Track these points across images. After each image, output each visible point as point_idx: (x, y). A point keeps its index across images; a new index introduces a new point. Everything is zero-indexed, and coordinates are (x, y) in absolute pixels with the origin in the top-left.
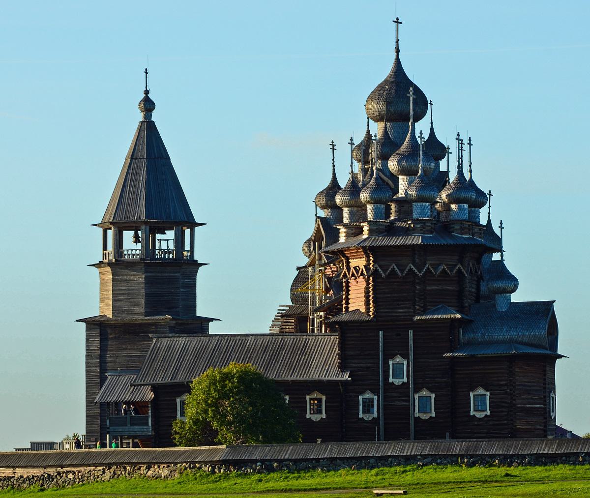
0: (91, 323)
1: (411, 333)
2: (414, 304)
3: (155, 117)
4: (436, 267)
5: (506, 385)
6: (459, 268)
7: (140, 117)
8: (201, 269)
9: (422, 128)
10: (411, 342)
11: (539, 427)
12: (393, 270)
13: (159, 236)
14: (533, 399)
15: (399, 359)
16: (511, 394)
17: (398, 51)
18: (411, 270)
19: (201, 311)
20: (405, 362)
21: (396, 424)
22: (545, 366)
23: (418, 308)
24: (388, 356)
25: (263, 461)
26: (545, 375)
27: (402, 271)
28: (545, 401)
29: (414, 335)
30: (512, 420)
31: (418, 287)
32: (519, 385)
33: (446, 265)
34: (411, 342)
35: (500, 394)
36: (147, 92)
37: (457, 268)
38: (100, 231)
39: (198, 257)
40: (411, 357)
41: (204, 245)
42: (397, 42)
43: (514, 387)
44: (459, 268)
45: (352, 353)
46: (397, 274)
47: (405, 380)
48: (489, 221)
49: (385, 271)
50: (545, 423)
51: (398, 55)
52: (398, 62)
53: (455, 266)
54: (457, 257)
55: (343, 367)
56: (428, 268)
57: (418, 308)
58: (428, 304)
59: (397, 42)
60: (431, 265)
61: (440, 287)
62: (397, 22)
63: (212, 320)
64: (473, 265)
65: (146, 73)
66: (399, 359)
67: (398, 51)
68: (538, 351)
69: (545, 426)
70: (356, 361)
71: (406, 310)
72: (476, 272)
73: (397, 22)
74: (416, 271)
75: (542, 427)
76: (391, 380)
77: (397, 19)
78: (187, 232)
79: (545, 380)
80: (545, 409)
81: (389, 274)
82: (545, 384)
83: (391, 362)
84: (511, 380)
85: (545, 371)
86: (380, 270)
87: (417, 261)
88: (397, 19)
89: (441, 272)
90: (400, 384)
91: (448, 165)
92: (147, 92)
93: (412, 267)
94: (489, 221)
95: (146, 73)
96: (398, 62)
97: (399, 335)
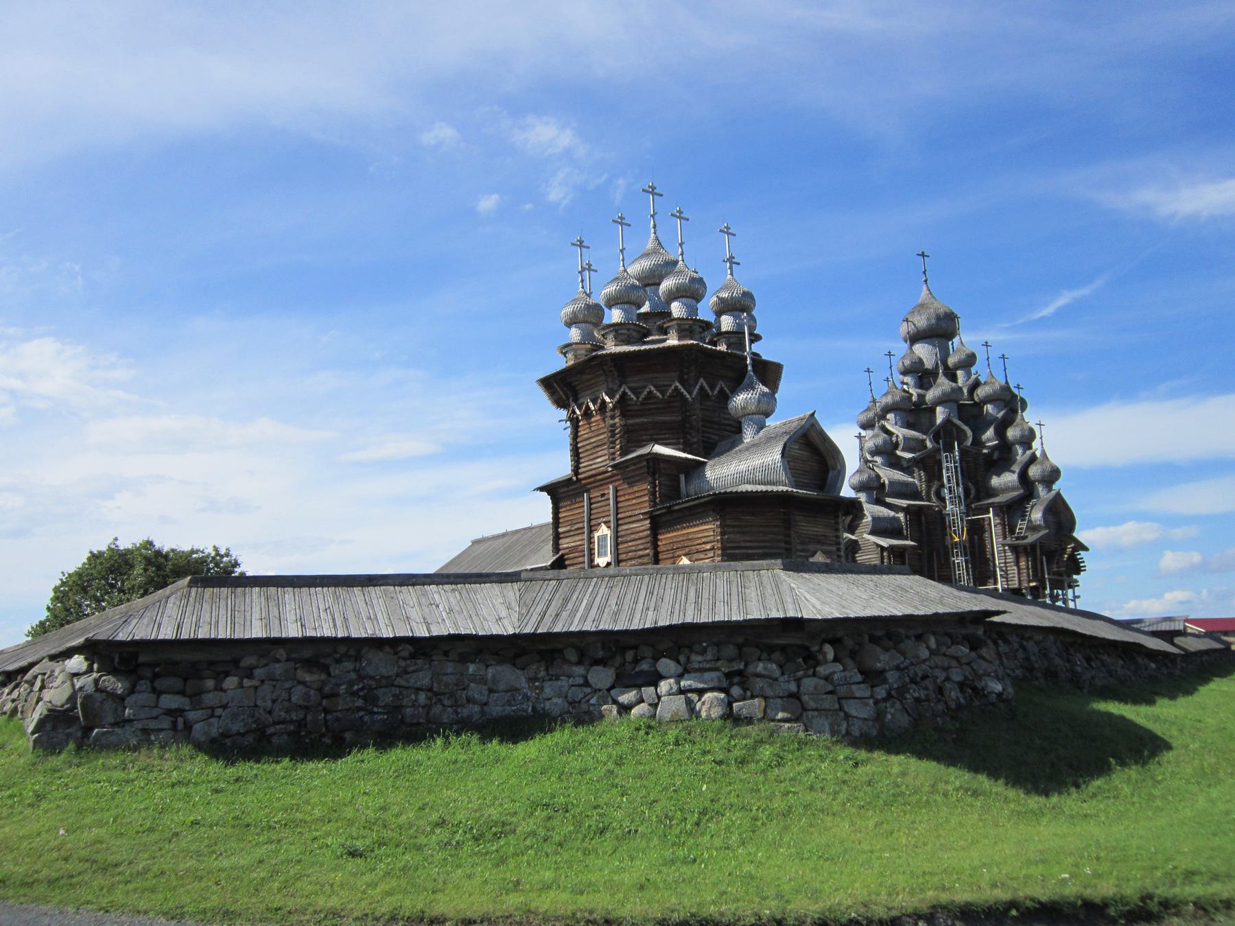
5: (713, 548)
6: (676, 389)
10: (611, 502)
26: (788, 528)
47: (608, 559)
55: (556, 548)
56: (624, 394)
60: (631, 389)
61: (650, 419)
62: (923, 255)
68: (775, 488)
73: (923, 255)
79: (788, 535)
83: (596, 535)
91: (980, 370)
97: (603, 495)
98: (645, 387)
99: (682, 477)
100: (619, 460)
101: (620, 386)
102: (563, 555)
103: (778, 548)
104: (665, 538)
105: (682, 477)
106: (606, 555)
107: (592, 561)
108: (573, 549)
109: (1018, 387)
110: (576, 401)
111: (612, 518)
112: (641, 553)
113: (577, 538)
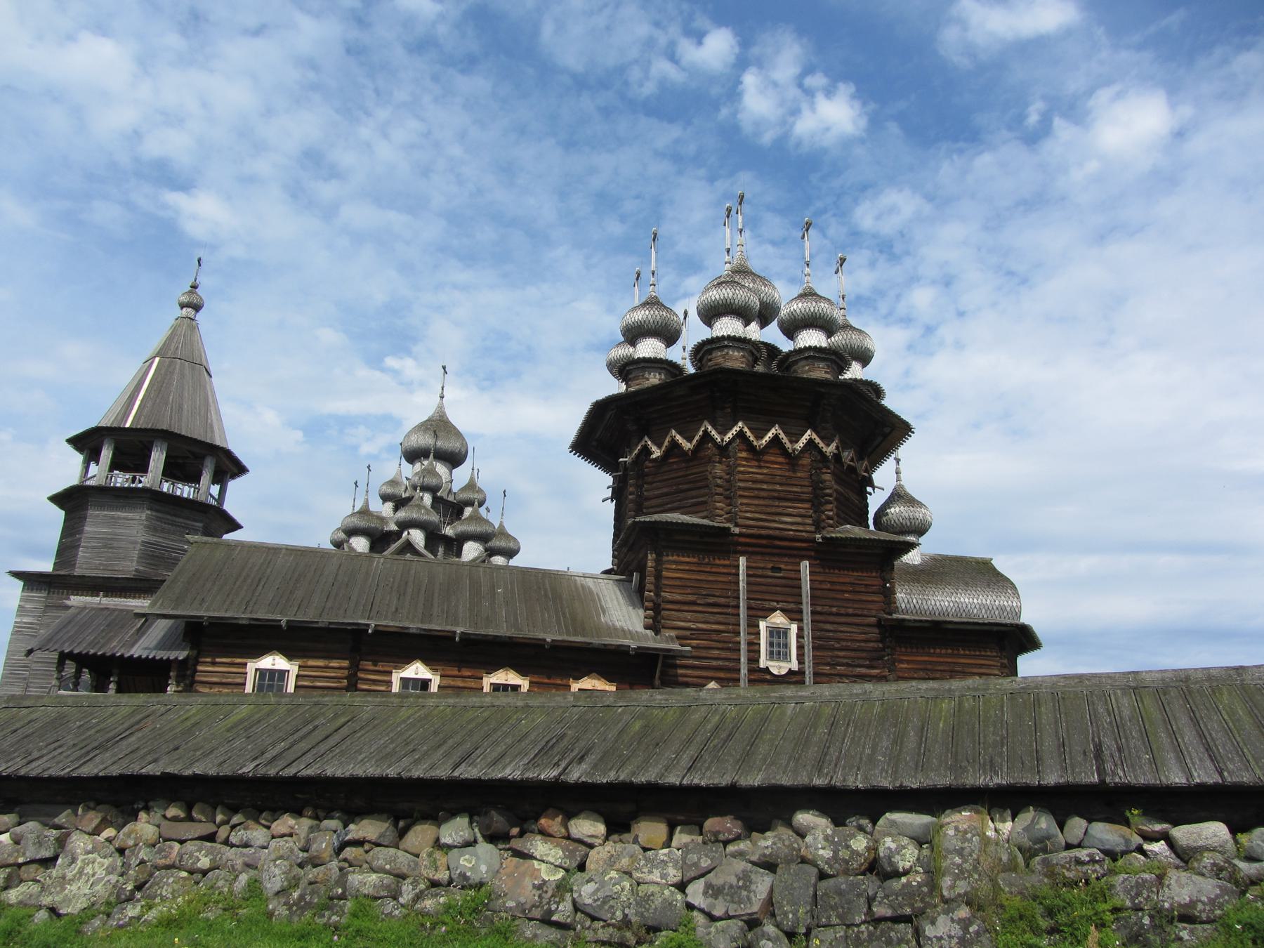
1: (805, 566)
3: (200, 317)
9: (461, 476)
15: (778, 619)
17: (442, 397)
20: (794, 628)
24: (758, 612)
36: (194, 287)
40: (807, 618)
45: (678, 597)
47: (794, 665)
66: (778, 619)
67: (442, 397)
70: (689, 616)
71: (798, 520)
76: (763, 662)
83: (763, 625)
86: (749, 434)
90: (784, 672)
97: (780, 570)
106: (786, 657)
107: (754, 658)
111: (807, 609)
113: (720, 618)
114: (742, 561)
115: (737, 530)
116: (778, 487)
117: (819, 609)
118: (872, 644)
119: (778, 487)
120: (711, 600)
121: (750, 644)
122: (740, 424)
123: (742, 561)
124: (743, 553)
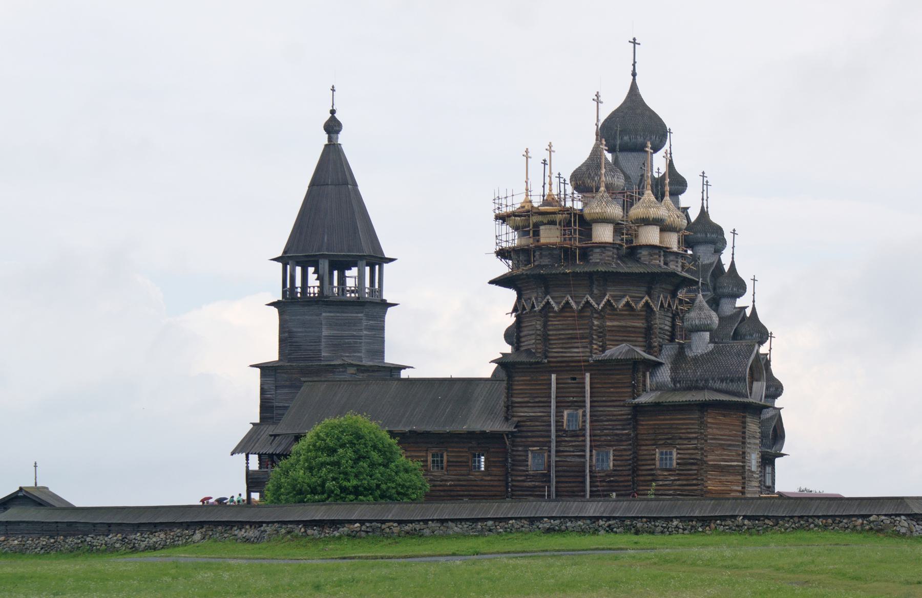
0: (266, 369)
2: (591, 343)
3: (342, 139)
4: (618, 298)
5: (696, 438)
7: (324, 139)
8: (390, 309)
10: (588, 388)
11: (736, 488)
12: (568, 303)
13: (348, 273)
14: (729, 455)
16: (702, 449)
17: (634, 74)
18: (588, 302)
19: (390, 358)
21: (571, 483)
22: (744, 417)
23: (595, 347)
25: (362, 522)
26: (744, 428)
27: (577, 303)
28: (744, 458)
29: (591, 378)
30: (702, 480)
31: (596, 323)
32: (712, 439)
33: (630, 297)
34: (588, 388)
35: (689, 449)
36: (333, 112)
37: (644, 300)
38: (280, 265)
39: (388, 296)
41: (394, 284)
42: (634, 65)
43: (706, 441)
44: (647, 302)
45: (519, 400)
46: (571, 307)
48: (733, 264)
49: (558, 303)
50: (744, 483)
51: (634, 79)
52: (634, 88)
53: (643, 298)
54: (644, 289)
56: (608, 301)
57: (595, 347)
58: (608, 343)
59: (634, 65)
61: (622, 323)
62: (634, 42)
63: (404, 368)
64: (666, 298)
65: (333, 90)
67: (634, 74)
69: (743, 488)
70: (526, 409)
72: (669, 305)
73: (634, 42)
74: (594, 303)
75: (740, 488)
77: (634, 39)
78: (377, 267)
79: (744, 433)
80: (743, 467)
81: (563, 307)
82: (744, 438)
84: (701, 433)
85: (744, 423)
86: (552, 303)
87: (596, 291)
88: (634, 39)
89: (625, 306)
91: (690, 200)
92: (333, 112)
93: (590, 299)
94: (733, 264)
95: (333, 90)
96: (634, 88)
97: (574, 379)
98: (624, 296)
99: (648, 374)
100: (601, 357)
101: (605, 295)
102: (519, 422)
103: (738, 441)
104: (646, 423)
105: (648, 374)
108: (532, 419)
109: (734, 232)
110: (547, 293)
112: (618, 432)
113: (541, 410)
114: (554, 376)
115: (546, 361)
116: (571, 332)
117: (595, 399)
118: (625, 417)
119: (571, 332)
120: (537, 400)
121: (557, 422)
122: (548, 297)
123: (554, 376)
124: (554, 372)
